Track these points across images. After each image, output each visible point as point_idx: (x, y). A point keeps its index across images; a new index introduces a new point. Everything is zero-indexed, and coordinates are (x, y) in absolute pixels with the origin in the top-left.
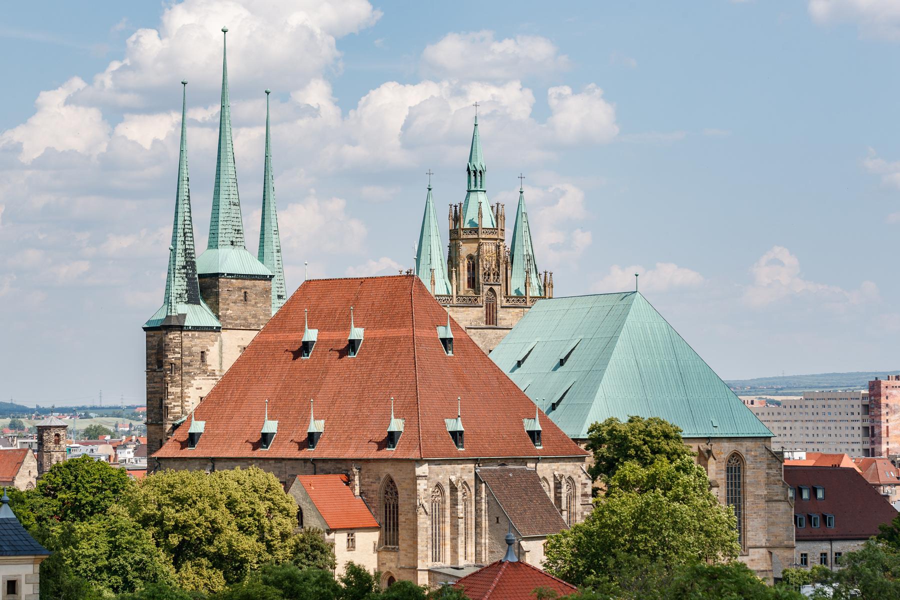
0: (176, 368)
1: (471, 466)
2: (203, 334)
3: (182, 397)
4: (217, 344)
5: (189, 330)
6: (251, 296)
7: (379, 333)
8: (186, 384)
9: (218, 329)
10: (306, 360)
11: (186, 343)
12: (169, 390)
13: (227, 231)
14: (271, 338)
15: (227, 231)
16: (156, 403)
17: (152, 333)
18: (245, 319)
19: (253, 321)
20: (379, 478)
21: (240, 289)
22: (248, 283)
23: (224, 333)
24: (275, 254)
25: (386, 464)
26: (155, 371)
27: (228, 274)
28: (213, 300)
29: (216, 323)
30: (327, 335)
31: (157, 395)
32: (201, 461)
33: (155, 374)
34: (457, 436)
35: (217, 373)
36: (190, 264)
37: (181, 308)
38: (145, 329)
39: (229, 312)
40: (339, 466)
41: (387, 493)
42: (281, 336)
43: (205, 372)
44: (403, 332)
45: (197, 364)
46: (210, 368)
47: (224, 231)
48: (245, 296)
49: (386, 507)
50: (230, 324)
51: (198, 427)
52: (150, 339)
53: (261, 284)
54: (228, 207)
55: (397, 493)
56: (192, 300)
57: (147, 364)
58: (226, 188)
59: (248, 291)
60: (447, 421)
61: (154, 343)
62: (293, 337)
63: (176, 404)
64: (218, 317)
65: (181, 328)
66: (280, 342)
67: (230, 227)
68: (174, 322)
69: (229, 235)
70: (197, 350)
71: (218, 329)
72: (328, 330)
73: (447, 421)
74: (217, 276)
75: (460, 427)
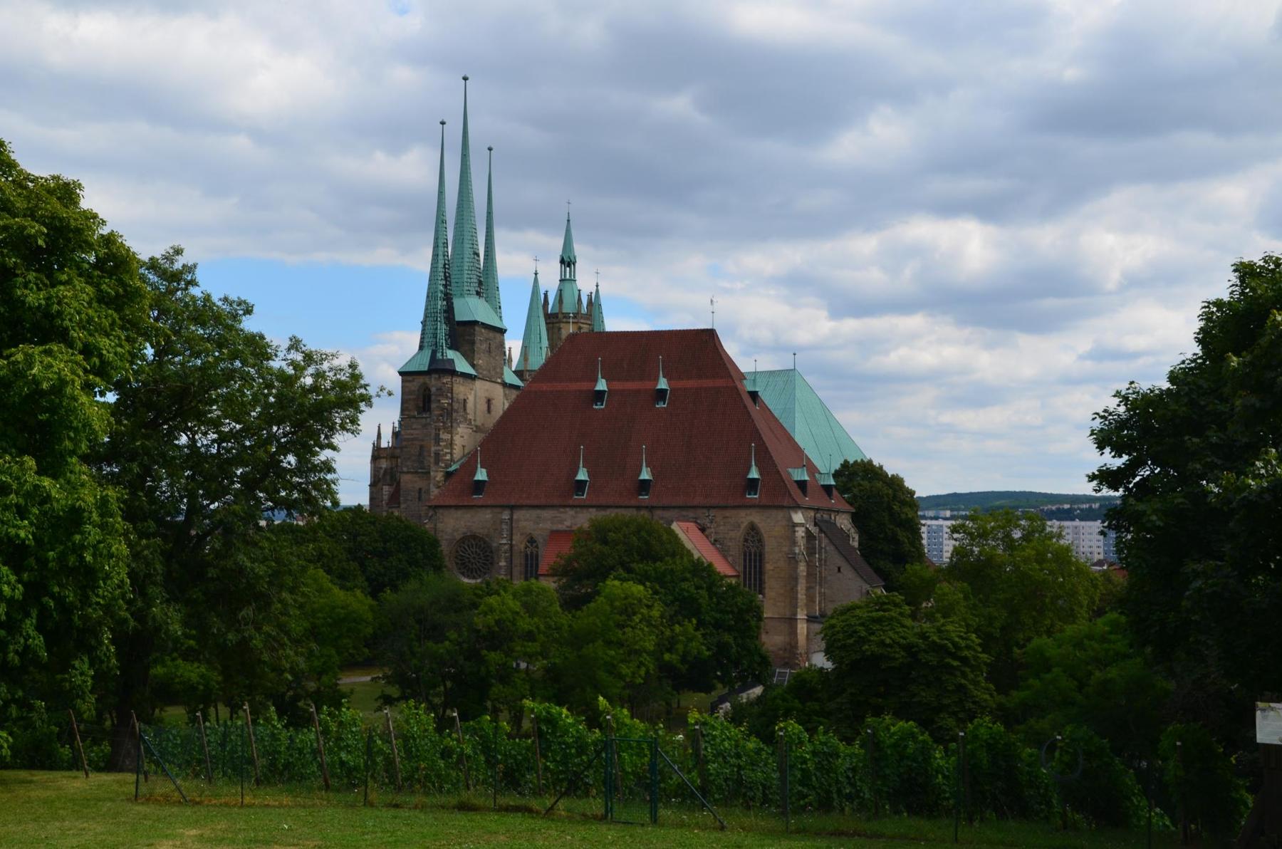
1: (812, 514)
3: (451, 444)
6: (493, 347)
7: (690, 384)
14: (545, 387)
21: (487, 339)
22: (491, 335)
23: (478, 383)
30: (618, 385)
34: (802, 485)
36: (449, 310)
37: (451, 354)
38: (401, 373)
40: (684, 513)
41: (746, 540)
44: (720, 383)
51: (481, 475)
53: (498, 335)
55: (760, 541)
62: (574, 386)
64: (473, 366)
65: (453, 373)
74: (476, 323)
75: (807, 478)
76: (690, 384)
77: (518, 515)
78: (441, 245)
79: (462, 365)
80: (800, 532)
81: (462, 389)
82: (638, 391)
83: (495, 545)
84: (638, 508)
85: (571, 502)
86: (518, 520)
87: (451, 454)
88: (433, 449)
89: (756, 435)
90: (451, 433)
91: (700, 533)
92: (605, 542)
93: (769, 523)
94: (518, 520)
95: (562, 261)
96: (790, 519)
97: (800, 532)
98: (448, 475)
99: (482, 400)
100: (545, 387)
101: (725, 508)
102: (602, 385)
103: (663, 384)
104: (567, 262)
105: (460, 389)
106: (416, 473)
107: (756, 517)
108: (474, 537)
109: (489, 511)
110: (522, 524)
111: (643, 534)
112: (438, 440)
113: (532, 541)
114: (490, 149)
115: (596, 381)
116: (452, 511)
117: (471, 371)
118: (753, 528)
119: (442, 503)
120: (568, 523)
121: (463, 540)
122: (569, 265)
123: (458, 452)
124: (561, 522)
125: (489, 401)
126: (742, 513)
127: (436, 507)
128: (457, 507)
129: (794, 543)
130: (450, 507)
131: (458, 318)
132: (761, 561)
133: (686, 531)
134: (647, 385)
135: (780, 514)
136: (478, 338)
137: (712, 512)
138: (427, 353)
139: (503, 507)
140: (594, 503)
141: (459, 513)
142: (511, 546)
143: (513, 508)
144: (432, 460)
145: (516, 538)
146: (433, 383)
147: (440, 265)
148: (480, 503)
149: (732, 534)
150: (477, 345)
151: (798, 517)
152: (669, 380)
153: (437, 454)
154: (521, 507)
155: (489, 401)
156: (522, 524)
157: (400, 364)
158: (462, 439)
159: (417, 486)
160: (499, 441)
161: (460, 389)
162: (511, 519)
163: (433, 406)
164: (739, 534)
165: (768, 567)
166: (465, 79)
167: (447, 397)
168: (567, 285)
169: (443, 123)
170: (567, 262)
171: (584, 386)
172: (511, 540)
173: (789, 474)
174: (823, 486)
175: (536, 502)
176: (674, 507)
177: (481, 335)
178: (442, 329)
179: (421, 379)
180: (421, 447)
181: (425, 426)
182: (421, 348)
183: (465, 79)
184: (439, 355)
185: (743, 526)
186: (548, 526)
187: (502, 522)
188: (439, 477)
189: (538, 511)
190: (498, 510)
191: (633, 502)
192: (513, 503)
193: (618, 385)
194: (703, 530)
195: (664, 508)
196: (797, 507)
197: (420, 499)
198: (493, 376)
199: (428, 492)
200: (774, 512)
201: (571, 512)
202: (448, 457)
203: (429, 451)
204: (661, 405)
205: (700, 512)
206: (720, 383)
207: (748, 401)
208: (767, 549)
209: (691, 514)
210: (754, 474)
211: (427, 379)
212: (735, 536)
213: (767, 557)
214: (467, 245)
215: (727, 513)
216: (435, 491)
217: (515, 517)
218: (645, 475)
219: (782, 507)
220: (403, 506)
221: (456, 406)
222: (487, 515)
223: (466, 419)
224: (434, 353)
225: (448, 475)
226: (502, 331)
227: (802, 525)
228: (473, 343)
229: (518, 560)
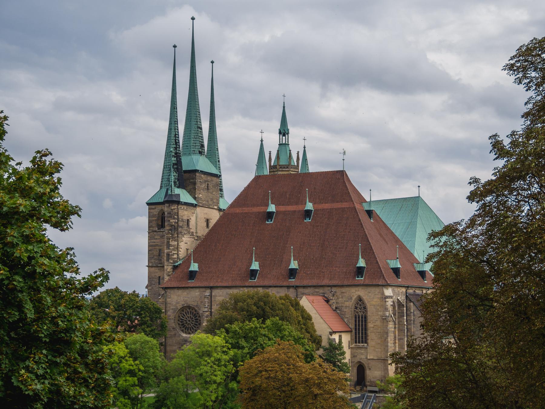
0: (175, 229)
1: (404, 290)
2: (188, 207)
3: (177, 248)
4: (194, 215)
5: (182, 204)
6: (211, 186)
7: (327, 206)
8: (180, 240)
9: (195, 206)
10: (270, 224)
11: (181, 213)
12: (170, 243)
13: (196, 144)
14: (238, 210)
15: (196, 144)
16: (156, 253)
17: (153, 207)
18: (208, 201)
19: (210, 203)
20: (351, 299)
21: (206, 181)
22: (209, 178)
23: (198, 209)
24: (217, 163)
25: (357, 289)
26: (156, 231)
27: (201, 171)
28: (191, 187)
29: (194, 202)
30: (282, 208)
31: (157, 247)
33: (155, 233)
34: (396, 271)
35: (194, 234)
36: (178, 164)
37: (177, 191)
38: (148, 204)
39: (201, 195)
40: (317, 290)
41: (356, 308)
42: (246, 210)
43: (189, 232)
44: (345, 205)
45: (185, 227)
46: (191, 230)
47: (194, 144)
48: (208, 187)
49: (356, 318)
50: (201, 203)
51: (194, 267)
52: (152, 211)
53: (215, 179)
54: (197, 129)
55: (365, 308)
56: (181, 185)
57: (149, 227)
58: (195, 118)
59: (209, 183)
60: (388, 261)
61: (155, 213)
62: (256, 210)
63: (175, 252)
64: (195, 198)
65: (178, 203)
66: (246, 213)
67: (198, 142)
68: (174, 199)
69: (198, 147)
70: (185, 218)
71: (195, 206)
72: (283, 205)
73: (388, 261)
74: (196, 171)
75: (399, 266)
76: (327, 206)
77: (215, 292)
78: (173, 123)
79: (185, 196)
80: (389, 302)
81: (186, 213)
82: (294, 212)
83: (201, 312)
84: (288, 287)
85: (247, 284)
86: (215, 296)
87: (178, 255)
88: (166, 251)
89: (365, 239)
90: (178, 241)
91: (325, 303)
93: (370, 297)
95: (280, 133)
96: (383, 293)
97: (389, 302)
98: (175, 268)
99: (200, 219)
101: (342, 286)
102: (272, 208)
103: (309, 206)
104: (284, 132)
105: (184, 213)
106: (157, 267)
107: (361, 292)
108: (189, 307)
109: (197, 290)
111: (262, 304)
112: (168, 245)
114: (212, 62)
115: (267, 205)
116: (176, 291)
117: (192, 201)
118: (360, 299)
119: (169, 286)
121: (183, 309)
122: (284, 135)
123: (182, 253)
125: (207, 221)
126: (353, 290)
127: (166, 288)
128: (178, 288)
129: (386, 309)
131: (184, 168)
132: (366, 321)
133: (312, 302)
134: (299, 208)
135: (377, 290)
136: (198, 181)
137: (334, 290)
138: (164, 190)
140: (261, 284)
141: (180, 292)
143: (211, 288)
144: (165, 258)
145: (215, 308)
146: (166, 208)
147: (173, 135)
148: (192, 285)
149: (347, 304)
150: (198, 185)
151: (388, 292)
152: (314, 204)
153: (168, 255)
154: (217, 287)
155: (207, 221)
157: (147, 198)
158: (185, 244)
160: (206, 247)
161: (184, 213)
162: (211, 295)
163: (166, 224)
164: (350, 304)
165: (370, 325)
167: (174, 218)
168: (283, 147)
169: (175, 47)
170: (284, 132)
171: (261, 209)
172: (211, 309)
173: (388, 264)
174: (419, 272)
176: (310, 286)
177: (200, 179)
178: (173, 176)
179: (159, 207)
180: (160, 250)
182: (161, 187)
184: (169, 192)
185: (354, 298)
190: (204, 290)
191: (285, 284)
192: (211, 285)
193: (282, 208)
194: (327, 301)
195: (304, 287)
196: (387, 285)
198: (212, 204)
199: (163, 279)
200: (373, 289)
202: (175, 256)
204: (308, 220)
206: (345, 205)
207: (364, 217)
208: (369, 314)
209: (321, 290)
210: (361, 263)
212: (349, 305)
213: (369, 319)
214: (193, 123)
215: (344, 290)
216: (167, 278)
217: (213, 294)
218: (294, 265)
219: (378, 286)
221: (181, 224)
222: (196, 293)
223: (189, 232)
226: (218, 176)
227: (391, 297)
228: (195, 184)
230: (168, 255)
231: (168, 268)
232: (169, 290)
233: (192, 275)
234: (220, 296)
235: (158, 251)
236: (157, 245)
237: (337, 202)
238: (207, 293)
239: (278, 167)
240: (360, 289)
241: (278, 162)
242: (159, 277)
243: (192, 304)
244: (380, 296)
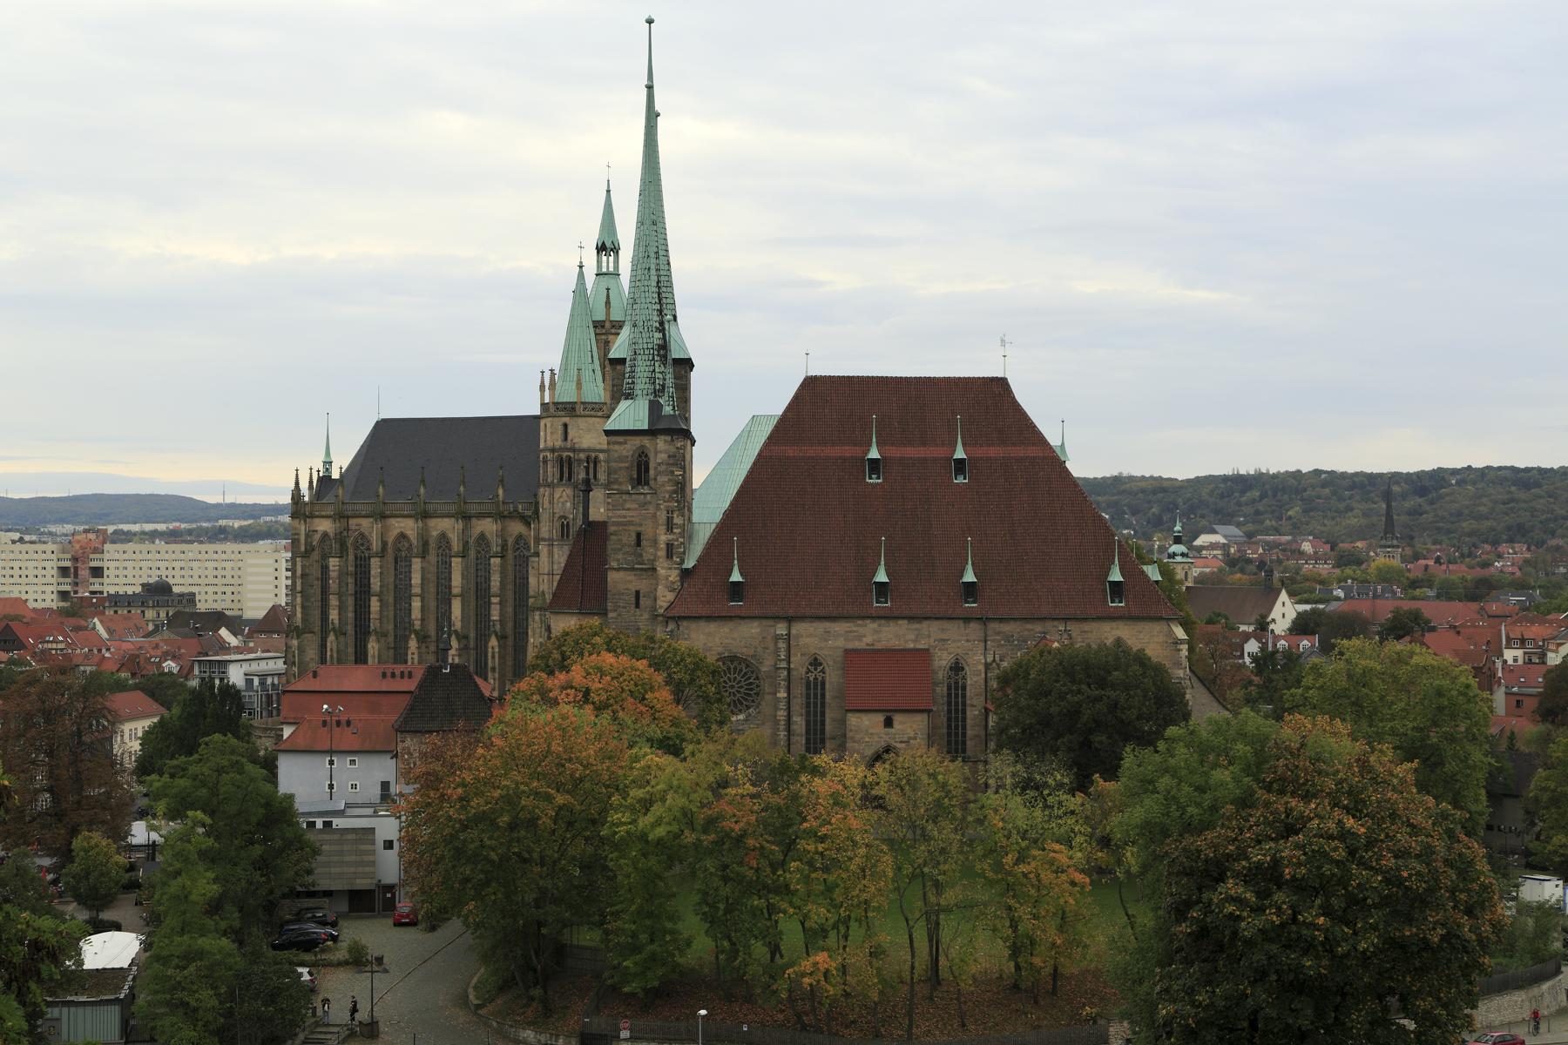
7: (994, 452)
14: (791, 451)
25: (1114, 624)
30: (894, 452)
32: (765, 622)
40: (1029, 626)
76: (994, 452)
77: (799, 628)
82: (925, 459)
84: (967, 620)
86: (798, 636)
92: (1102, 683)
94: (798, 636)
98: (686, 574)
100: (791, 451)
106: (633, 569)
108: (733, 658)
110: (802, 641)
113: (816, 663)
115: (870, 445)
116: (702, 624)
120: (868, 639)
124: (860, 638)
128: (709, 618)
130: (699, 618)
135: (1157, 628)
139: (777, 618)
142: (789, 670)
143: (790, 620)
144: (662, 553)
145: (796, 660)
146: (661, 447)
148: (738, 612)
154: (803, 618)
156: (804, 641)
159: (633, 587)
162: (789, 635)
166: (650, 22)
171: (848, 451)
172: (789, 663)
175: (822, 612)
179: (636, 441)
180: (639, 535)
181: (644, 505)
183: (650, 22)
186: (841, 643)
187: (777, 638)
188: (674, 576)
189: (827, 625)
190: (771, 622)
192: (791, 612)
193: (894, 452)
195: (1001, 620)
197: (637, 605)
201: (872, 625)
203: (655, 542)
204: (960, 480)
205: (1049, 624)
206: (1032, 451)
211: (646, 441)
215: (1086, 626)
217: (793, 632)
219: (1159, 619)
220: (611, 615)
222: (752, 630)
224: (655, 408)
225: (686, 574)
229: (799, 690)
230: (670, 547)
231: (667, 573)
232: (685, 623)
233: (736, 590)
234: (810, 636)
235: (634, 536)
236: (630, 523)
237: (1014, 444)
238: (781, 629)
239: (608, 325)
240: (1121, 624)
241: (608, 314)
242: (638, 593)
243: (743, 652)
244: (1161, 639)
